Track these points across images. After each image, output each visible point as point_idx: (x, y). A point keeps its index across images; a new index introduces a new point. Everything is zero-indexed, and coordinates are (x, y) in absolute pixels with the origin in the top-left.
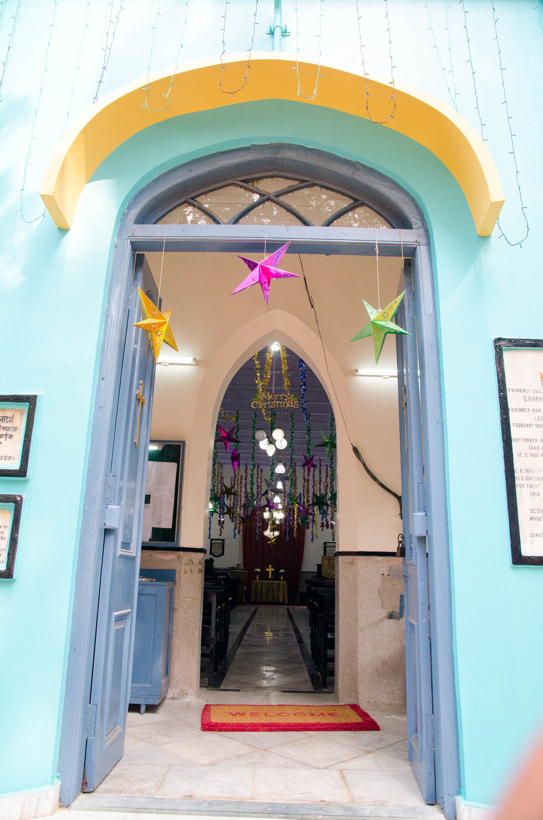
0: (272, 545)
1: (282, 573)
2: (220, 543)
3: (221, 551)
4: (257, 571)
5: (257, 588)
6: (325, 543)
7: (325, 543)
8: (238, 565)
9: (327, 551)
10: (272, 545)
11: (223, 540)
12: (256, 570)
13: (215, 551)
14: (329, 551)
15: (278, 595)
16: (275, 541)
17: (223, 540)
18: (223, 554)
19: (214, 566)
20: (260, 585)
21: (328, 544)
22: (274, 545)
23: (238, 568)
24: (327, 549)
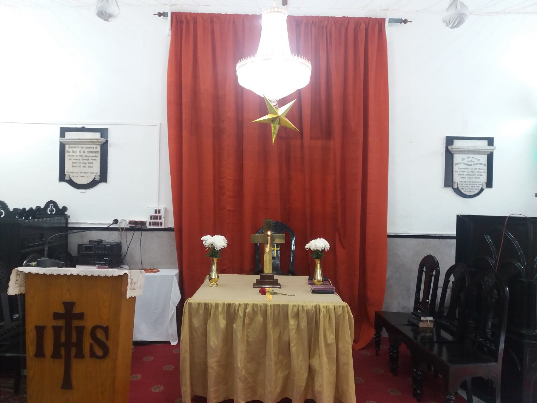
0: (275, 129)
1: (318, 254)
2: (92, 142)
3: (96, 169)
4: (212, 248)
5: (205, 334)
6: (450, 141)
7: (450, 141)
8: (156, 216)
9: (456, 168)
10: (275, 129)
11: (104, 132)
12: (208, 240)
13: (76, 170)
14: (462, 166)
15: (311, 372)
16: (289, 115)
17: (104, 132)
18: (103, 177)
19: (71, 220)
20: (222, 323)
21: (458, 144)
22: (283, 129)
23: (157, 224)
24: (457, 158)
